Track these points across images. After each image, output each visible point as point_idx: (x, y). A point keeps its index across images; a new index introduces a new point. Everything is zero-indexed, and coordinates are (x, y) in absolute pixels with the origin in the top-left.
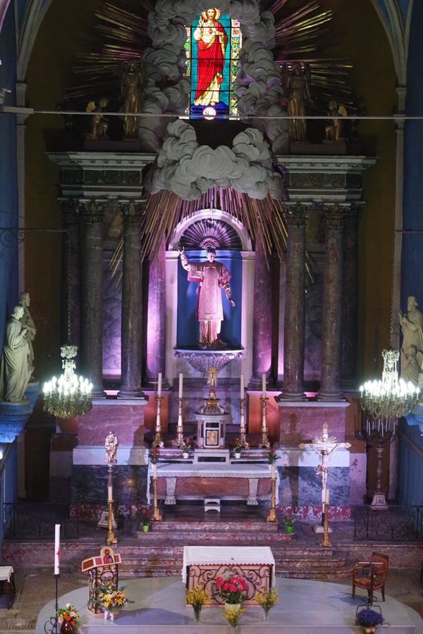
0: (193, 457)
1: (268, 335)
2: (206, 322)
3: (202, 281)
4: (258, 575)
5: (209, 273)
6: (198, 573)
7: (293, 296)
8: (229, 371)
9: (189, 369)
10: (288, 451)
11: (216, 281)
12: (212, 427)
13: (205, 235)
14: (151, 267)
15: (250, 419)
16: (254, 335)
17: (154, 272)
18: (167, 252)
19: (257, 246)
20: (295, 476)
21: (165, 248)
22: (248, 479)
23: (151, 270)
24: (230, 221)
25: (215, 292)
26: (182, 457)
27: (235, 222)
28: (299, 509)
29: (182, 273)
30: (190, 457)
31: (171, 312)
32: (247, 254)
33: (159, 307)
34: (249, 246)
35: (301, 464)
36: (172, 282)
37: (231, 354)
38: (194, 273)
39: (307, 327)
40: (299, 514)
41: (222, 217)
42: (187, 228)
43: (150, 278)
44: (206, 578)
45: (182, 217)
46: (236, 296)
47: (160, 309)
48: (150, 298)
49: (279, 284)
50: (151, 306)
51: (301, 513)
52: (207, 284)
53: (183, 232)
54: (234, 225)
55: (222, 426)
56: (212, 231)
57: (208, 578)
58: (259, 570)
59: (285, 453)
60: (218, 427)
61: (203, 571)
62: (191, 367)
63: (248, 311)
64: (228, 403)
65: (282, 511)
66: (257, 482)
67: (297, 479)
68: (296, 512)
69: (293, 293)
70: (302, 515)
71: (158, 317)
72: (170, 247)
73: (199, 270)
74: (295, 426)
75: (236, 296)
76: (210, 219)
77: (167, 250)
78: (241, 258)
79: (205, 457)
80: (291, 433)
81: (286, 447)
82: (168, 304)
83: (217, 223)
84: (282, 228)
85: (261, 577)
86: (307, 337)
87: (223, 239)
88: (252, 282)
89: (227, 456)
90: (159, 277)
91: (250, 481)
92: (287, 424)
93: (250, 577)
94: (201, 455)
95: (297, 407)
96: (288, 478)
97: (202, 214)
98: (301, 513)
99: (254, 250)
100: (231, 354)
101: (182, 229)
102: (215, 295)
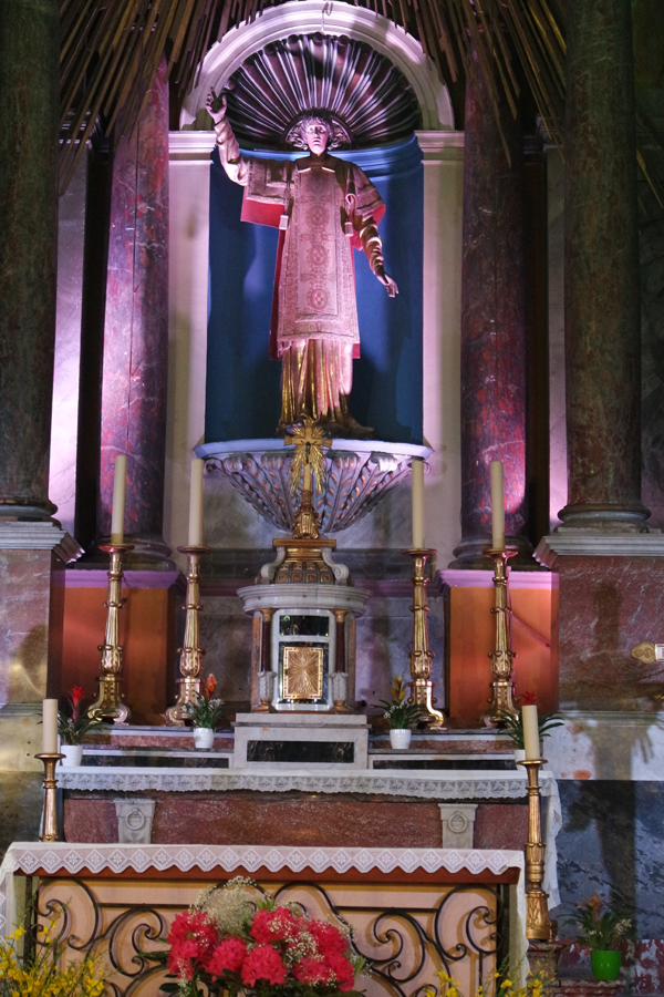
0: (228, 745)
1: (511, 387)
2: (302, 344)
3: (289, 214)
4: (430, 942)
5: (309, 188)
6: (83, 927)
7: (591, 162)
8: (383, 525)
9: (246, 521)
10: (592, 723)
11: (333, 212)
12: (301, 632)
13: (303, 105)
14: (117, 167)
15: (455, 675)
16: (463, 395)
17: (127, 181)
18: (172, 135)
19: (469, 103)
20: (621, 819)
21: (166, 120)
22: (435, 802)
23: (116, 176)
24: (383, 40)
25: (330, 245)
26: (190, 744)
27: (399, 40)
28: (640, 949)
29: (224, 195)
30: (218, 745)
31: (188, 328)
32: (438, 140)
33: (140, 294)
34: (445, 113)
35: (641, 773)
36: (192, 232)
37: (388, 456)
38: (260, 188)
39: (647, 362)
40: (640, 970)
41: (356, 27)
42: (239, 62)
43: (113, 204)
44: (126, 955)
45: (224, 22)
46: (402, 257)
47: (145, 300)
48: (112, 268)
49: (546, 220)
50: (114, 292)
51: (647, 964)
52: (302, 220)
53: (227, 74)
54: (395, 49)
55: (340, 628)
56: (324, 93)
57: (142, 958)
58: (436, 912)
59: (580, 729)
60: (323, 631)
61: (110, 915)
62: (254, 512)
63: (442, 305)
64: (379, 637)
65: (576, 955)
66: (472, 816)
67: (631, 828)
68: (629, 964)
69: (592, 153)
70: (653, 973)
71: (137, 327)
72: (186, 118)
73: (276, 178)
74: (614, 627)
75: (402, 257)
76: (318, 37)
77: (175, 126)
78: (421, 155)
79: (275, 744)
80: (603, 658)
81: (581, 708)
82: (177, 303)
83: (341, 53)
84: (551, 33)
85: (445, 957)
86: (647, 391)
87: (362, 119)
88: (454, 232)
89: (360, 739)
90: (142, 199)
91: (446, 812)
92: (586, 623)
93: (386, 950)
94: (257, 735)
95: (618, 560)
96: (593, 828)
97: (291, 17)
98: (647, 964)
99: (459, 125)
100: (388, 456)
101: (224, 66)
102: (331, 255)
